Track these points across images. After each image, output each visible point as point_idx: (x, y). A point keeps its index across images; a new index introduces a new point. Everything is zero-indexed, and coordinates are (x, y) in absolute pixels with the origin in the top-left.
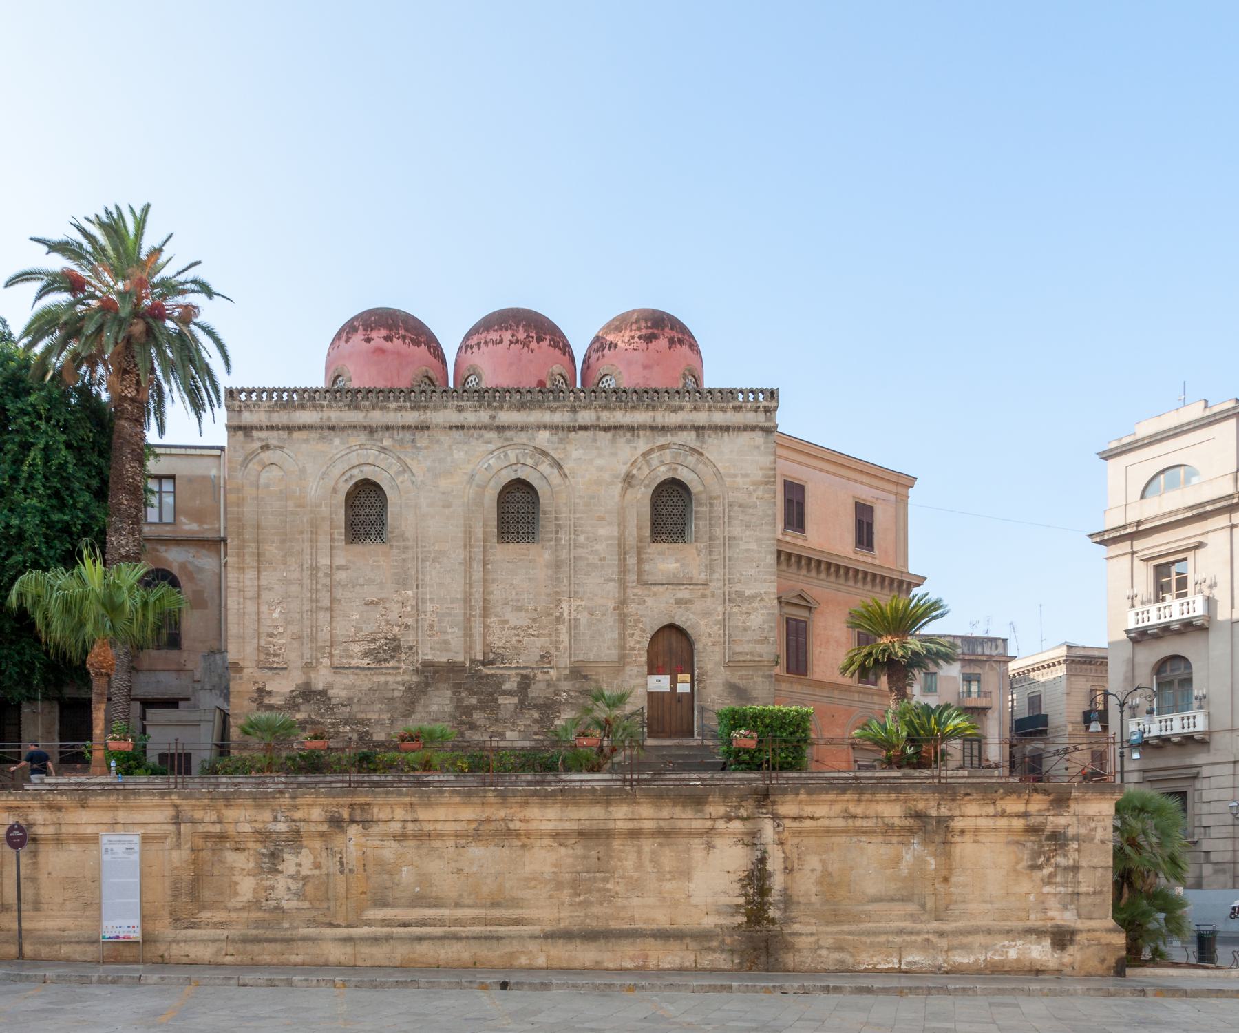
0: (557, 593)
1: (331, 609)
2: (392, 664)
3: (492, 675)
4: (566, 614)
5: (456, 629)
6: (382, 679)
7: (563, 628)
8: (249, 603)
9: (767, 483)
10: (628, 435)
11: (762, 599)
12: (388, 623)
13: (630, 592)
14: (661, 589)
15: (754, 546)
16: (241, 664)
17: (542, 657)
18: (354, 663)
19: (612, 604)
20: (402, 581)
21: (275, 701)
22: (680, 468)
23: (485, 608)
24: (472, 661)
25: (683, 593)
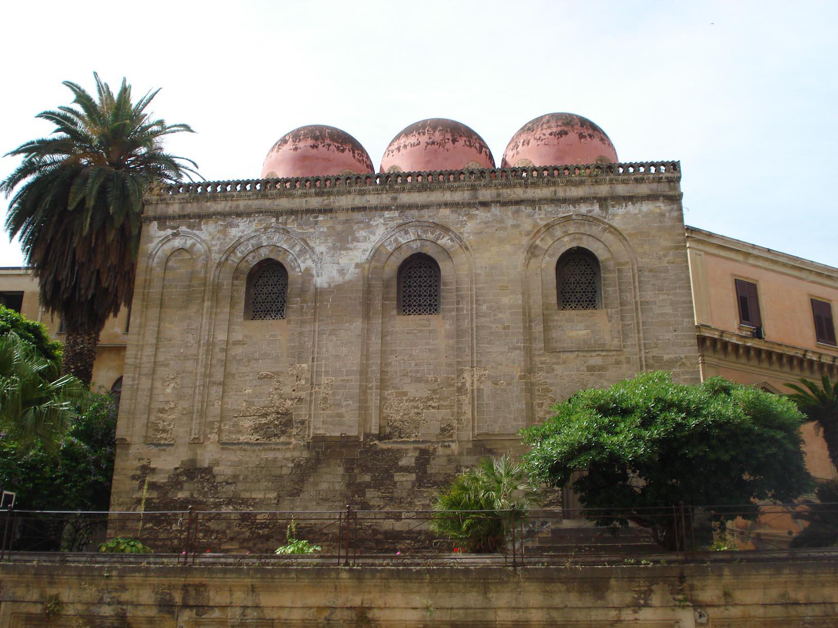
0: (459, 363)
1: (223, 384)
2: (282, 439)
3: (388, 450)
4: (468, 385)
5: (350, 402)
6: (271, 455)
7: (466, 399)
8: (144, 379)
9: (677, 248)
10: (529, 210)
11: (683, 364)
12: (281, 396)
13: (537, 359)
14: (571, 356)
15: (669, 310)
16: (128, 439)
17: (443, 430)
18: (243, 438)
19: (518, 373)
20: (298, 355)
21: (161, 479)
22: (585, 237)
23: (381, 379)
24: (367, 436)
25: (595, 360)
